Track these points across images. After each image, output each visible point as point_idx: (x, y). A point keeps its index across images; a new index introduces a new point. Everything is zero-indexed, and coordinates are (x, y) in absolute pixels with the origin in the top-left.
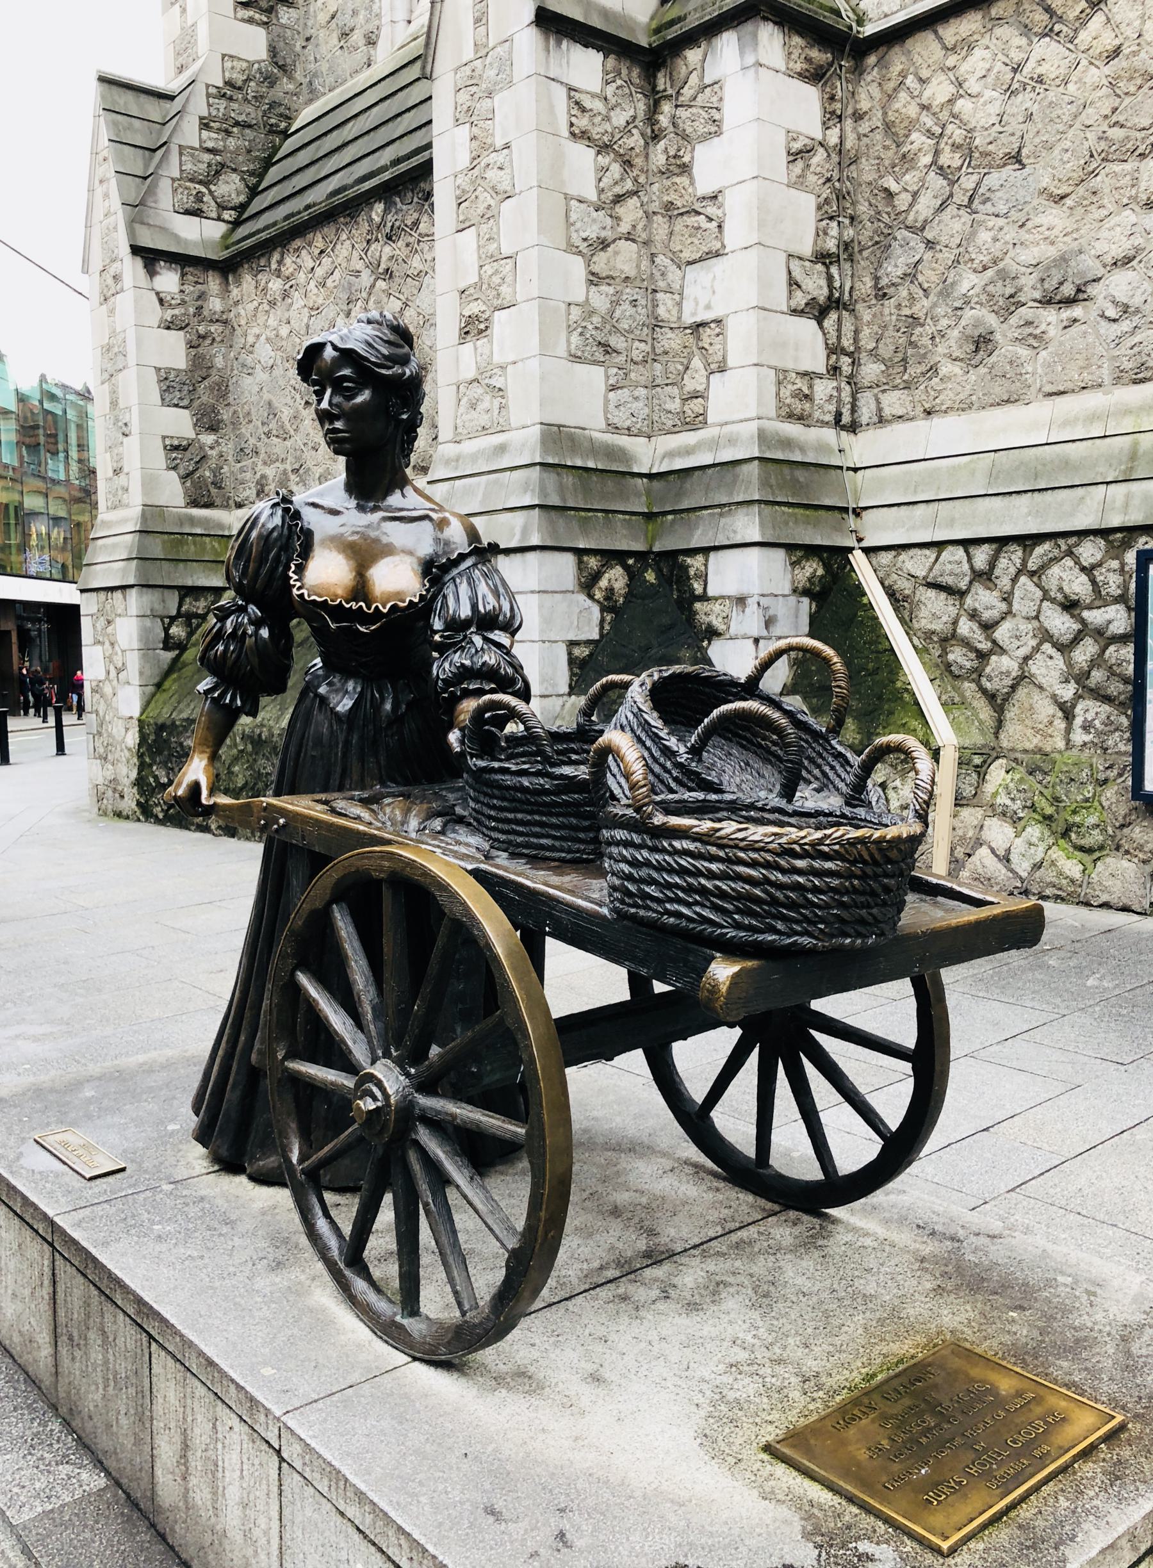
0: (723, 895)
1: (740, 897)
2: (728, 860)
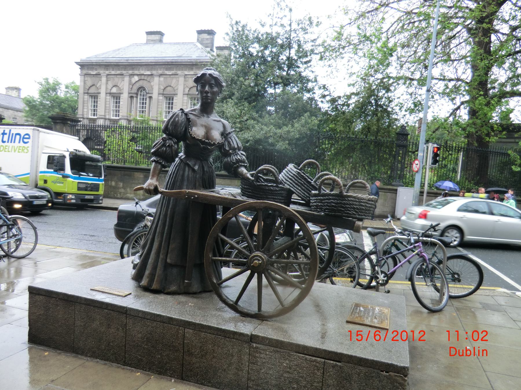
0: (358, 209)
1: (361, 209)
2: (359, 202)
